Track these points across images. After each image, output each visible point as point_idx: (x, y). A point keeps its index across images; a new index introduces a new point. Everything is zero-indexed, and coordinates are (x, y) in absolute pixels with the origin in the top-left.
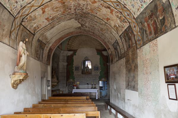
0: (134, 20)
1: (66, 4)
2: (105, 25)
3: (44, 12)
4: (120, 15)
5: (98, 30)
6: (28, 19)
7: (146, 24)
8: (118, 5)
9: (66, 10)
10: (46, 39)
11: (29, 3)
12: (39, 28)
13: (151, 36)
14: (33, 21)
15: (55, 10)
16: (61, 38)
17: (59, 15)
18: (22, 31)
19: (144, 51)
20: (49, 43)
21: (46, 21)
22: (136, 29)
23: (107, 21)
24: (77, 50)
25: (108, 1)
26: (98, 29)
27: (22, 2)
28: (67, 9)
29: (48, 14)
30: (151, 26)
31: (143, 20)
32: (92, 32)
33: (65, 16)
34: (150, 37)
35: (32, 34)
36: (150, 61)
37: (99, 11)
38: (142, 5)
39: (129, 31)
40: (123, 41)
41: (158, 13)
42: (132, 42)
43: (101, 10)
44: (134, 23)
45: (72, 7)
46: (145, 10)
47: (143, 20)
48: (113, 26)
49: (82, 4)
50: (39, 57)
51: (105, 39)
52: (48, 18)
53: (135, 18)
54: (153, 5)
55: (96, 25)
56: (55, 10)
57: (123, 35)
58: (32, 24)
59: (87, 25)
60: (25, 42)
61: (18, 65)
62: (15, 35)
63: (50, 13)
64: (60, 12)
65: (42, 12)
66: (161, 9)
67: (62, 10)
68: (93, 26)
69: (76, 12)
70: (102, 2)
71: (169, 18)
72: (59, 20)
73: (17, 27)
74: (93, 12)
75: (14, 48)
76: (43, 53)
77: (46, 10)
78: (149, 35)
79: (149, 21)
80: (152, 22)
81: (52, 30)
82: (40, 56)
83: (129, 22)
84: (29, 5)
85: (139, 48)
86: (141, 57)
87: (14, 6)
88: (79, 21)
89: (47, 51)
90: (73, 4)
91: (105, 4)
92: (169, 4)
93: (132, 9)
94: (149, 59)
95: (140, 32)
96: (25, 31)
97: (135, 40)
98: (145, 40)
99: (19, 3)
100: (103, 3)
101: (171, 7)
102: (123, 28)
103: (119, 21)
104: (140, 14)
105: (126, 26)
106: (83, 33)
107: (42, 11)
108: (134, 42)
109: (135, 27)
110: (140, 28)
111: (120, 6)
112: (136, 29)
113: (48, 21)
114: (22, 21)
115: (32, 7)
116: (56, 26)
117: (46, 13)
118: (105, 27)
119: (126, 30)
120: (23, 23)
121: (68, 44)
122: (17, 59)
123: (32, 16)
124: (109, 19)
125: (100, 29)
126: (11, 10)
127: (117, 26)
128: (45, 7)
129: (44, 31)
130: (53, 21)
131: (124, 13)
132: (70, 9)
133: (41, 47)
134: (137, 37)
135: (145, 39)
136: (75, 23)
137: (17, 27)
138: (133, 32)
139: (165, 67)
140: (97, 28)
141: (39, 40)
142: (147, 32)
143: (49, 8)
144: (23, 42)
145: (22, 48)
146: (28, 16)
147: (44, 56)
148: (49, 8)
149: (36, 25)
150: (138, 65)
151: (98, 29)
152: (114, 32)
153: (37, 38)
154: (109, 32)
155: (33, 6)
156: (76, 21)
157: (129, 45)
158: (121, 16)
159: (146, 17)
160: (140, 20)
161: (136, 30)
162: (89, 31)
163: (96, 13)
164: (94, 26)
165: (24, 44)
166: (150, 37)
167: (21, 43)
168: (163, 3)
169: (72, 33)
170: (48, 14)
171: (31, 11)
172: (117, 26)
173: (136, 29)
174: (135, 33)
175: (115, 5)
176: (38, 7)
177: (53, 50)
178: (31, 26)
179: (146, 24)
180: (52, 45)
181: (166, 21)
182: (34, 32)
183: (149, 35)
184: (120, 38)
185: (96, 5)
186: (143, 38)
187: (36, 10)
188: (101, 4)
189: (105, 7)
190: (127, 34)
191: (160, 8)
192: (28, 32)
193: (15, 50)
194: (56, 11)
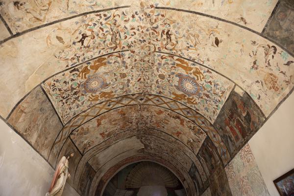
0: (212, 128)
1: (126, 115)
2: (175, 142)
3: (99, 124)
4: (192, 126)
5: (166, 152)
6: (79, 132)
7: (228, 128)
8: (188, 113)
10: (97, 164)
11: (84, 112)
12: (90, 146)
13: (239, 142)
15: (113, 123)
16: (117, 165)
18: (69, 146)
19: (234, 166)
20: (101, 172)
21: (100, 137)
22: (217, 139)
23: (178, 136)
24: (139, 189)
25: (176, 110)
26: (167, 150)
27: (76, 109)
28: (127, 123)
29: (104, 128)
30: (235, 129)
31: (223, 124)
32: (159, 157)
33: (125, 132)
34: (238, 144)
35: (81, 153)
36: (248, 179)
37: (167, 124)
38: (217, 106)
39: (208, 144)
40: (202, 162)
41: (239, 110)
42: (214, 159)
43: (169, 121)
44: (212, 131)
46: (223, 110)
47: (223, 124)
48: (185, 141)
49: (145, 117)
50: (84, 191)
51: (177, 164)
52: (103, 133)
53: (212, 124)
54: (230, 102)
55: (164, 144)
56: (113, 123)
57: (200, 152)
58: (82, 140)
59: (152, 145)
60: (69, 157)
61: (50, 192)
62: (58, 149)
63: (106, 126)
64: (119, 127)
65: (96, 124)
66: (241, 105)
67: (121, 123)
68: (161, 147)
69: (138, 127)
70: (170, 111)
71: (255, 112)
72: (117, 136)
73: (64, 140)
74: (159, 126)
75: (52, 166)
76: (90, 185)
77: (102, 122)
78: (235, 141)
79: (231, 123)
80: (235, 123)
81: (107, 150)
82: (85, 188)
83: (206, 132)
84: (84, 114)
85: (226, 165)
86: (233, 177)
87: (66, 112)
88: (142, 140)
89: (97, 184)
90: (135, 116)
91: (174, 114)
92: (247, 96)
93: (207, 113)
94: (246, 177)
95: (222, 141)
96: (73, 148)
97: (219, 155)
98: (232, 151)
99: (72, 110)
100: (171, 112)
101: (252, 99)
102: (199, 142)
103: (192, 133)
104: (217, 117)
105: (203, 137)
106: (148, 159)
107: (97, 123)
108: (217, 158)
109: (214, 136)
110: (221, 137)
111: (191, 113)
112: (217, 139)
114: (71, 134)
115: (86, 116)
116: (113, 146)
118: (176, 145)
119: (203, 144)
120: (72, 137)
121: (127, 180)
122: (52, 184)
124: (180, 133)
125: (169, 150)
126: (62, 117)
127: (192, 141)
128: (102, 118)
129: (97, 152)
130: (109, 138)
131: (198, 121)
132: (131, 123)
133: (89, 176)
134: (220, 150)
135: (232, 149)
136: (137, 142)
137: (64, 140)
138: (213, 144)
139: (276, 182)
140: (165, 149)
141: (87, 164)
142: (232, 139)
143: (106, 120)
144: (67, 158)
145: (63, 165)
146: (80, 127)
147: (91, 190)
148: (106, 120)
149: (87, 141)
150: (232, 193)
151: (167, 150)
152: (189, 151)
153: (86, 161)
154: (182, 153)
155: (87, 115)
156: (139, 140)
157: (212, 165)
158: (194, 127)
159: (226, 119)
160: (219, 125)
161: (217, 140)
162: (155, 154)
163: (163, 127)
164: (162, 146)
165: (67, 161)
166: (238, 144)
167: (64, 158)
168: (241, 97)
169: (133, 158)
170: (104, 128)
171: (85, 121)
172: (192, 141)
173: (216, 139)
174: (217, 145)
175: (186, 113)
177: (105, 183)
178: (81, 141)
179: (228, 128)
180: (104, 175)
181: (252, 117)
182: (84, 151)
183: (235, 141)
184: (197, 159)
185: (162, 116)
186: (228, 149)
188: (168, 114)
189: (173, 117)
190: (206, 150)
191: (239, 103)
192: (76, 150)
193: (53, 170)
194: (114, 125)
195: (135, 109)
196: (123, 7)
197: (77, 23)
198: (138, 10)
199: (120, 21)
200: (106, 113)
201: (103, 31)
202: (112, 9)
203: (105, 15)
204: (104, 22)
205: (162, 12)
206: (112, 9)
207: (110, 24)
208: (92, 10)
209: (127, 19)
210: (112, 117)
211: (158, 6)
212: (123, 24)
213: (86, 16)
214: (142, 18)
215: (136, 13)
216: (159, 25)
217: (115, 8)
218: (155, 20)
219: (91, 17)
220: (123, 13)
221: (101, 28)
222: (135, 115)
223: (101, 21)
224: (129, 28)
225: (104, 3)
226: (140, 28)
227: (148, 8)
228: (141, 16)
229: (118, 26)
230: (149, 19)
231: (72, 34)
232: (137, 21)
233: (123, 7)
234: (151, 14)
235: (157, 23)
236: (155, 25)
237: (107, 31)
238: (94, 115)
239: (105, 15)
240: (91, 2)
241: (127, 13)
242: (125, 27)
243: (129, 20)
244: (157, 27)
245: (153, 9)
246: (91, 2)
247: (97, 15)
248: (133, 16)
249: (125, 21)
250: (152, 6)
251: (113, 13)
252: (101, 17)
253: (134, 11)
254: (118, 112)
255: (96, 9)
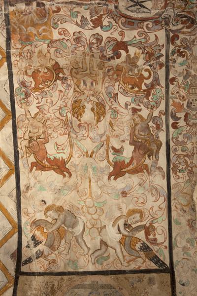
1: (62, 62)
3: (60, 167)
9: (118, 70)
14: (74, 225)
15: (88, 116)
17: (135, 111)
45: (105, 35)
56: (88, 116)
64: (123, 99)
65: (51, 176)
90: (83, 23)
113: (135, 171)
117: (76, 159)
123: (40, 216)
132: (123, 45)
176: (13, 177)
187: (22, 188)
195: (34, 25)
200: (20, 133)
210: (52, 113)
222: (72, 28)
238: (5, 171)
254: (36, 88)
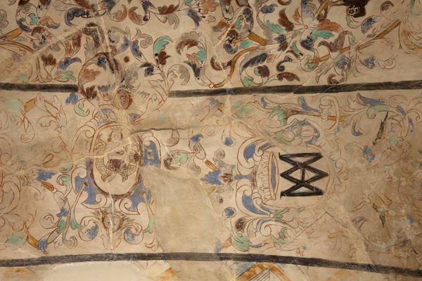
196: (197, 93)
197: (370, 63)
198: (142, 82)
199: (214, 45)
201: (282, 15)
202: (236, 91)
203: (264, 72)
204: (273, 48)
205: (51, 74)
206: (236, 91)
207: (252, 36)
208: (308, 96)
209: (186, 50)
211: (67, 95)
212: (205, 29)
213: (330, 79)
214: (129, 52)
215: (149, 70)
216: (63, 25)
217: (223, 92)
218: (78, 44)
219: (313, 74)
220: (197, 72)
221: (289, 27)
223: (282, 55)
224: (182, 15)
225: (259, 113)
226: (140, 12)
227: (104, 88)
228: (133, 59)
229: (223, 25)
230: (102, 49)
231: (398, 24)
232: (148, 40)
233: (197, 93)
234: (93, 67)
235: (73, 31)
236: (81, 23)
237: (268, 10)
239: (264, 72)
240: (304, 123)
241: (184, 72)
242: (197, 20)
243: (179, 48)
244: (71, 16)
245: (87, 85)
246: (304, 123)
247: (291, 76)
248: (162, 57)
249: (192, 43)
250: (90, 94)
251: (235, 76)
252: (280, 68)
253: (156, 76)
255: (292, 98)
